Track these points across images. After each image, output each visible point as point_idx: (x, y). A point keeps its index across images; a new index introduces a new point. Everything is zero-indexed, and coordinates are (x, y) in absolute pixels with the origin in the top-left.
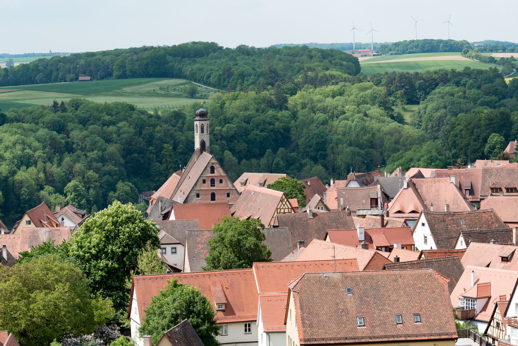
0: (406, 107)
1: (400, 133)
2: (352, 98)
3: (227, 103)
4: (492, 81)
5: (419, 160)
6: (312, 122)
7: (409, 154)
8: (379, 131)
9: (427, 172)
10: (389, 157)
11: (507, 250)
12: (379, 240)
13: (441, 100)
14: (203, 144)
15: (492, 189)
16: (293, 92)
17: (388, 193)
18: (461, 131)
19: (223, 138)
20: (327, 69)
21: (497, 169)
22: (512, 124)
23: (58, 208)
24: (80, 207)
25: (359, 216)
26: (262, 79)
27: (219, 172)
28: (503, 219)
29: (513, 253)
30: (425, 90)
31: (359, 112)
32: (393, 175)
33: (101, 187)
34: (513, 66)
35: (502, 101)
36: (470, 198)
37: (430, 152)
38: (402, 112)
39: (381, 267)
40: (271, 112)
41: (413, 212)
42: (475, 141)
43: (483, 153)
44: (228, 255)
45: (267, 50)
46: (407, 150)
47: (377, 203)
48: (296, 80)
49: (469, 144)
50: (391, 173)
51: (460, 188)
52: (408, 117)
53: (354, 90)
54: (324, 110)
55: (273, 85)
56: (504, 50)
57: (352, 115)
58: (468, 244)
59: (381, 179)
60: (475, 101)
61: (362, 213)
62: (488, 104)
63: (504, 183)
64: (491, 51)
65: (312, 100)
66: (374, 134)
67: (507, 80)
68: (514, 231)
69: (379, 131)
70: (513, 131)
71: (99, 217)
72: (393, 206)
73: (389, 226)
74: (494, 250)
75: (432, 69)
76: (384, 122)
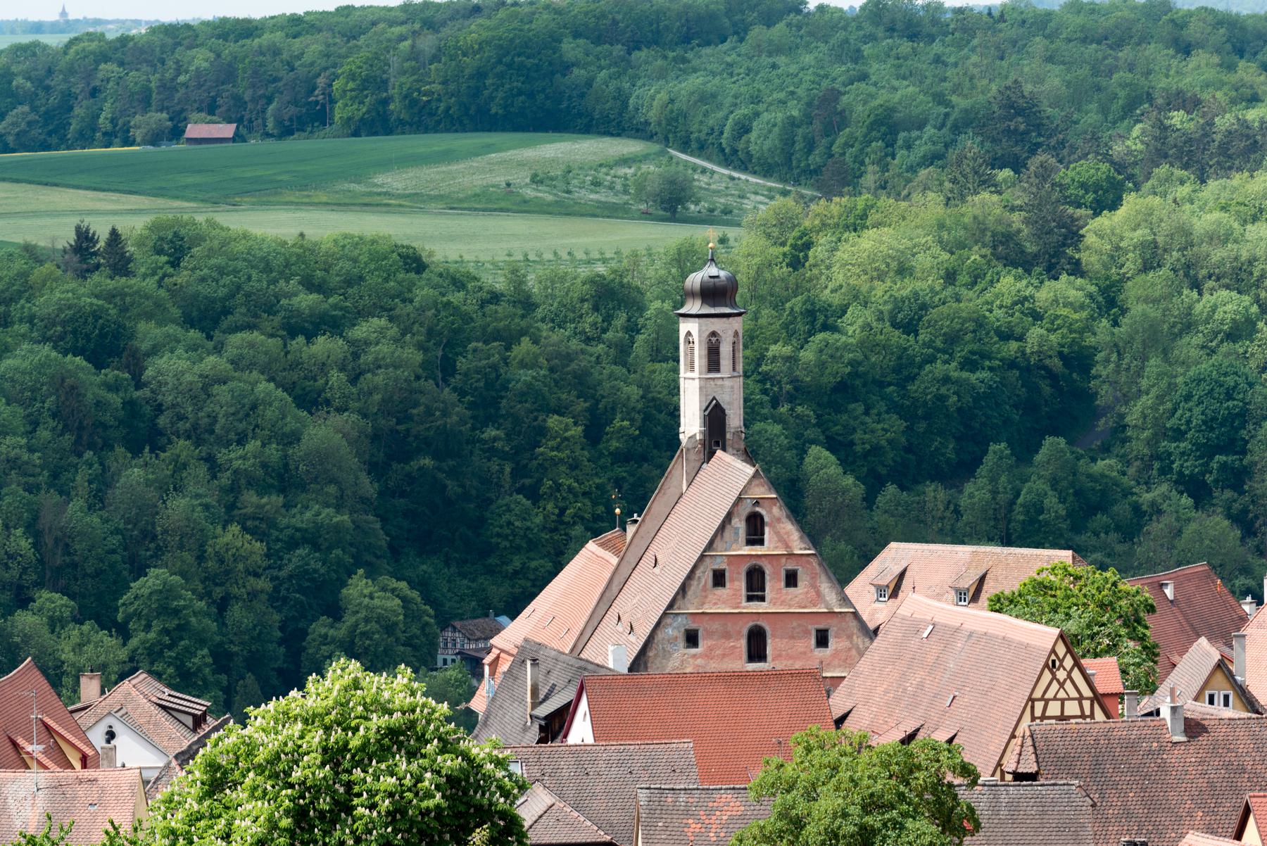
3: (821, 245)
6: (1188, 325)
14: (715, 417)
16: (1107, 199)
19: (799, 392)
23: (90, 687)
24: (184, 681)
26: (970, 144)
27: (784, 537)
33: (276, 599)
40: (1009, 284)
45: (994, 18)
48: (1118, 149)
54: (1239, 277)
55: (1017, 165)
65: (1185, 232)
71: (268, 726)
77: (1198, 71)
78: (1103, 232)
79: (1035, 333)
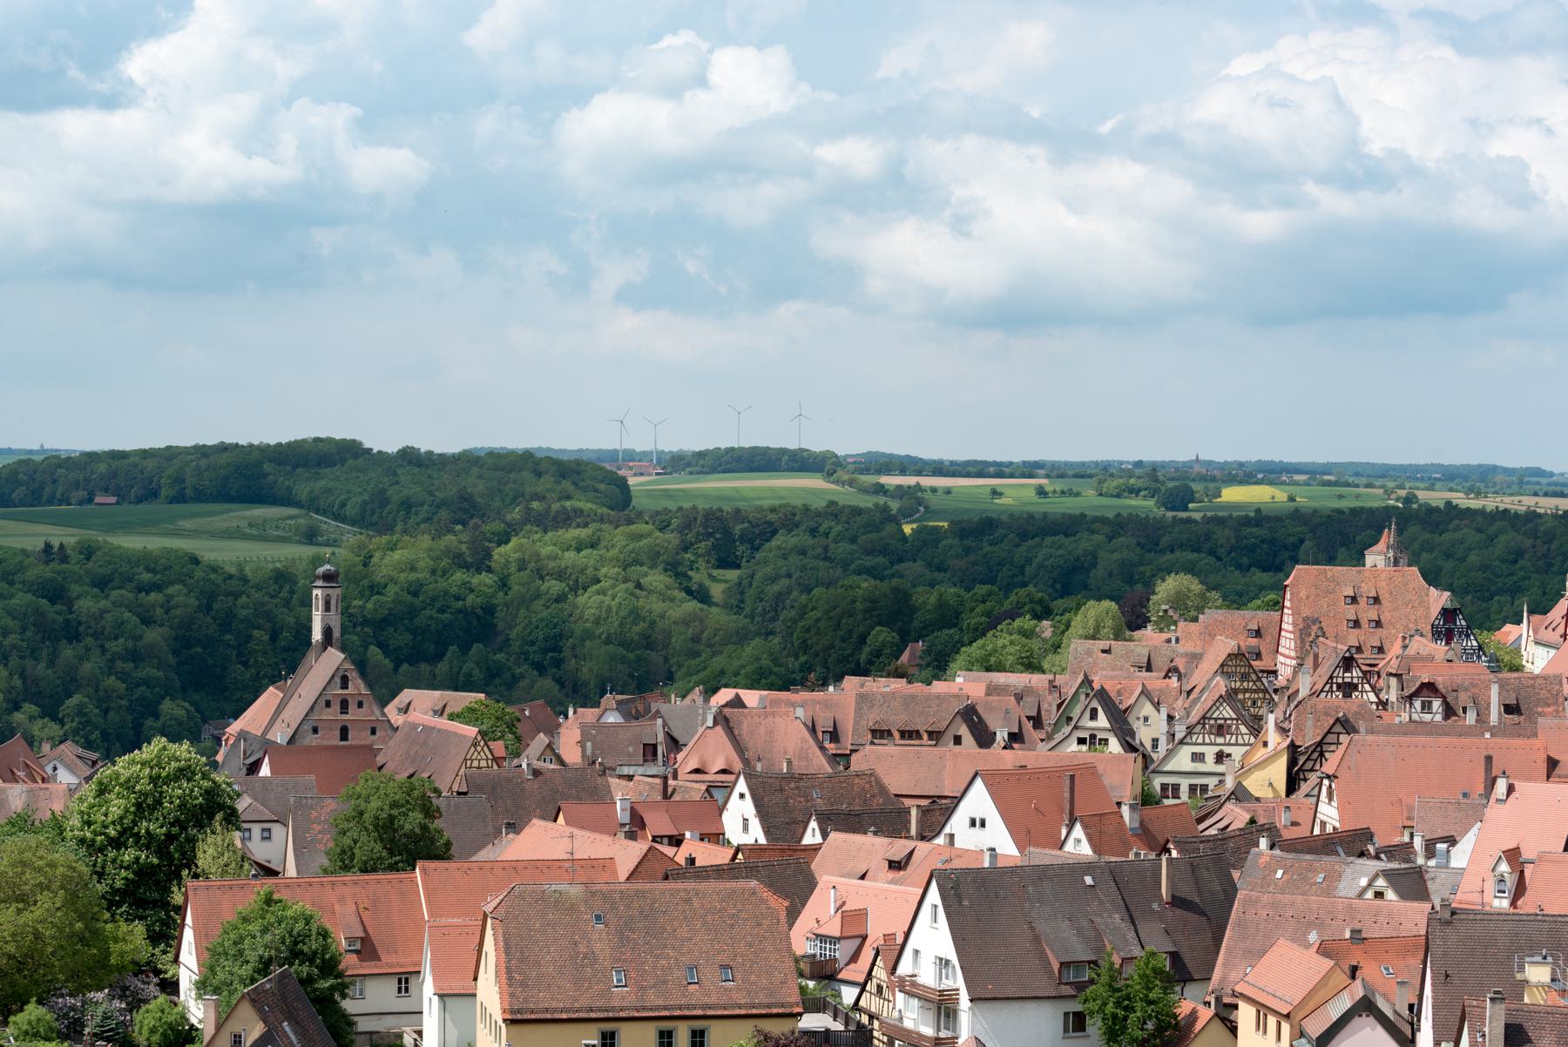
0: (715, 572)
1: (702, 621)
2: (613, 552)
3: (378, 555)
4: (878, 529)
5: (737, 674)
6: (538, 596)
7: (718, 662)
8: (662, 617)
9: (751, 697)
10: (680, 666)
11: (899, 848)
12: (658, 823)
13: (781, 563)
14: (327, 632)
15: (874, 732)
16: (504, 539)
17: (676, 734)
18: (817, 621)
19: (366, 622)
20: (569, 497)
21: (884, 695)
22: (914, 609)
23: (46, 747)
24: (88, 745)
25: (620, 777)
26: (444, 514)
27: (357, 686)
28: (893, 790)
29: (911, 854)
30: (751, 542)
31: (625, 581)
32: (689, 698)
33: (130, 709)
34: (920, 502)
35: (896, 567)
36: (831, 748)
37: (758, 659)
38: (708, 583)
39: (661, 874)
40: (459, 576)
41: (724, 771)
42: (843, 640)
43: (858, 664)
44: (369, 846)
46: (714, 654)
47: (655, 754)
48: (508, 517)
49: (832, 646)
50: (683, 697)
51: (813, 730)
52: (717, 591)
53: (618, 538)
54: (560, 575)
55: (464, 524)
56: (903, 471)
57: (613, 586)
58: (825, 835)
59: (664, 708)
60: (845, 565)
61: (626, 771)
62: (871, 572)
63: (896, 721)
64: (879, 472)
66: (653, 623)
67: (907, 529)
68: (914, 812)
69: (662, 617)
70: (916, 624)
71: (124, 766)
72: (687, 761)
73: (676, 797)
74: (874, 847)
75: (766, 503)
76: (672, 600)
77: (545, 484)
78: (500, 553)
79: (471, 598)
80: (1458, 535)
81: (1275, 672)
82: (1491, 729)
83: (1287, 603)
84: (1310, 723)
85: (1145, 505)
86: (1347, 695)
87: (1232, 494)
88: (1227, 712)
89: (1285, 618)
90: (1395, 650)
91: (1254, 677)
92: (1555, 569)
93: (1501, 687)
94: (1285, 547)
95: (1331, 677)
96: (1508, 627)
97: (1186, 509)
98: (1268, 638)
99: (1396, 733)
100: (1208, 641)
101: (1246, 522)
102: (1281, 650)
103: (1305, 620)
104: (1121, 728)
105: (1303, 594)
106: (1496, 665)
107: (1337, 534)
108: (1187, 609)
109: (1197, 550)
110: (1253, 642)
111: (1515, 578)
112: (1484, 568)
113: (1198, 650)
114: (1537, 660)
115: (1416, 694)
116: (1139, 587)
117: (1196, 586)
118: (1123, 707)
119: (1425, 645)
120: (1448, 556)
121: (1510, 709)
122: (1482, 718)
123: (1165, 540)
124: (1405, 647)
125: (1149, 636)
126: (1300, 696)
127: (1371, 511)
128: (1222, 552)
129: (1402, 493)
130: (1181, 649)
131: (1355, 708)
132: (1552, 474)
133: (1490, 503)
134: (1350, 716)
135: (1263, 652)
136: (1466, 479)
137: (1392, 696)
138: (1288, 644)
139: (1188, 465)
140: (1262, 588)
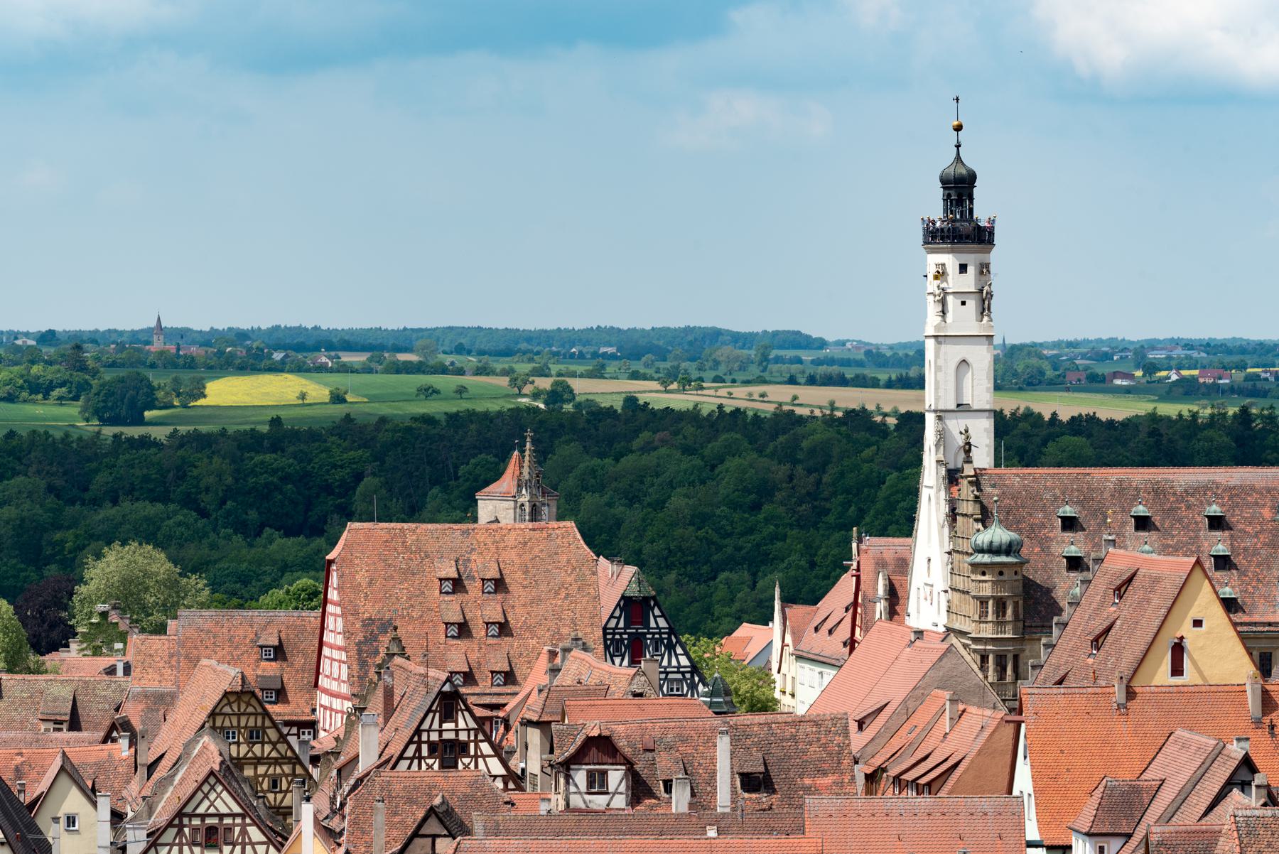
80: (649, 460)
81: (312, 725)
82: (718, 821)
83: (333, 595)
84: (380, 819)
85: (61, 416)
86: (449, 764)
87: (225, 392)
88: (224, 803)
89: (330, 622)
90: (535, 677)
91: (273, 734)
92: (831, 519)
93: (735, 742)
94: (328, 489)
95: (418, 731)
96: (745, 630)
97: (140, 421)
98: (299, 661)
99: (543, 833)
100: (187, 667)
101: (250, 442)
102: (323, 682)
103: (368, 623)
104: (22, 839)
105: (362, 577)
106: (725, 700)
107: (427, 465)
108: (142, 609)
109: (165, 499)
110: (271, 668)
111: (756, 537)
112: (700, 519)
113: (167, 687)
114: (801, 689)
115: (577, 758)
116: (52, 570)
117: (158, 563)
118: (26, 799)
119: (590, 666)
120: (632, 499)
121: (752, 782)
122: (700, 800)
123: (101, 480)
124: (555, 671)
125: (74, 662)
126: (361, 768)
127: (486, 417)
128: (207, 500)
129: (545, 383)
130: (135, 685)
131: (463, 789)
132: (822, 344)
133: (709, 399)
134: (454, 803)
135: (290, 687)
136: (662, 355)
137: (534, 764)
138: (336, 671)
139: (139, 338)
140: (285, 568)
